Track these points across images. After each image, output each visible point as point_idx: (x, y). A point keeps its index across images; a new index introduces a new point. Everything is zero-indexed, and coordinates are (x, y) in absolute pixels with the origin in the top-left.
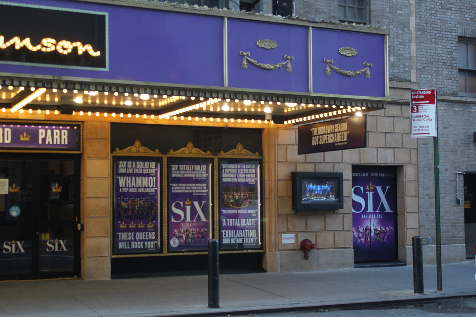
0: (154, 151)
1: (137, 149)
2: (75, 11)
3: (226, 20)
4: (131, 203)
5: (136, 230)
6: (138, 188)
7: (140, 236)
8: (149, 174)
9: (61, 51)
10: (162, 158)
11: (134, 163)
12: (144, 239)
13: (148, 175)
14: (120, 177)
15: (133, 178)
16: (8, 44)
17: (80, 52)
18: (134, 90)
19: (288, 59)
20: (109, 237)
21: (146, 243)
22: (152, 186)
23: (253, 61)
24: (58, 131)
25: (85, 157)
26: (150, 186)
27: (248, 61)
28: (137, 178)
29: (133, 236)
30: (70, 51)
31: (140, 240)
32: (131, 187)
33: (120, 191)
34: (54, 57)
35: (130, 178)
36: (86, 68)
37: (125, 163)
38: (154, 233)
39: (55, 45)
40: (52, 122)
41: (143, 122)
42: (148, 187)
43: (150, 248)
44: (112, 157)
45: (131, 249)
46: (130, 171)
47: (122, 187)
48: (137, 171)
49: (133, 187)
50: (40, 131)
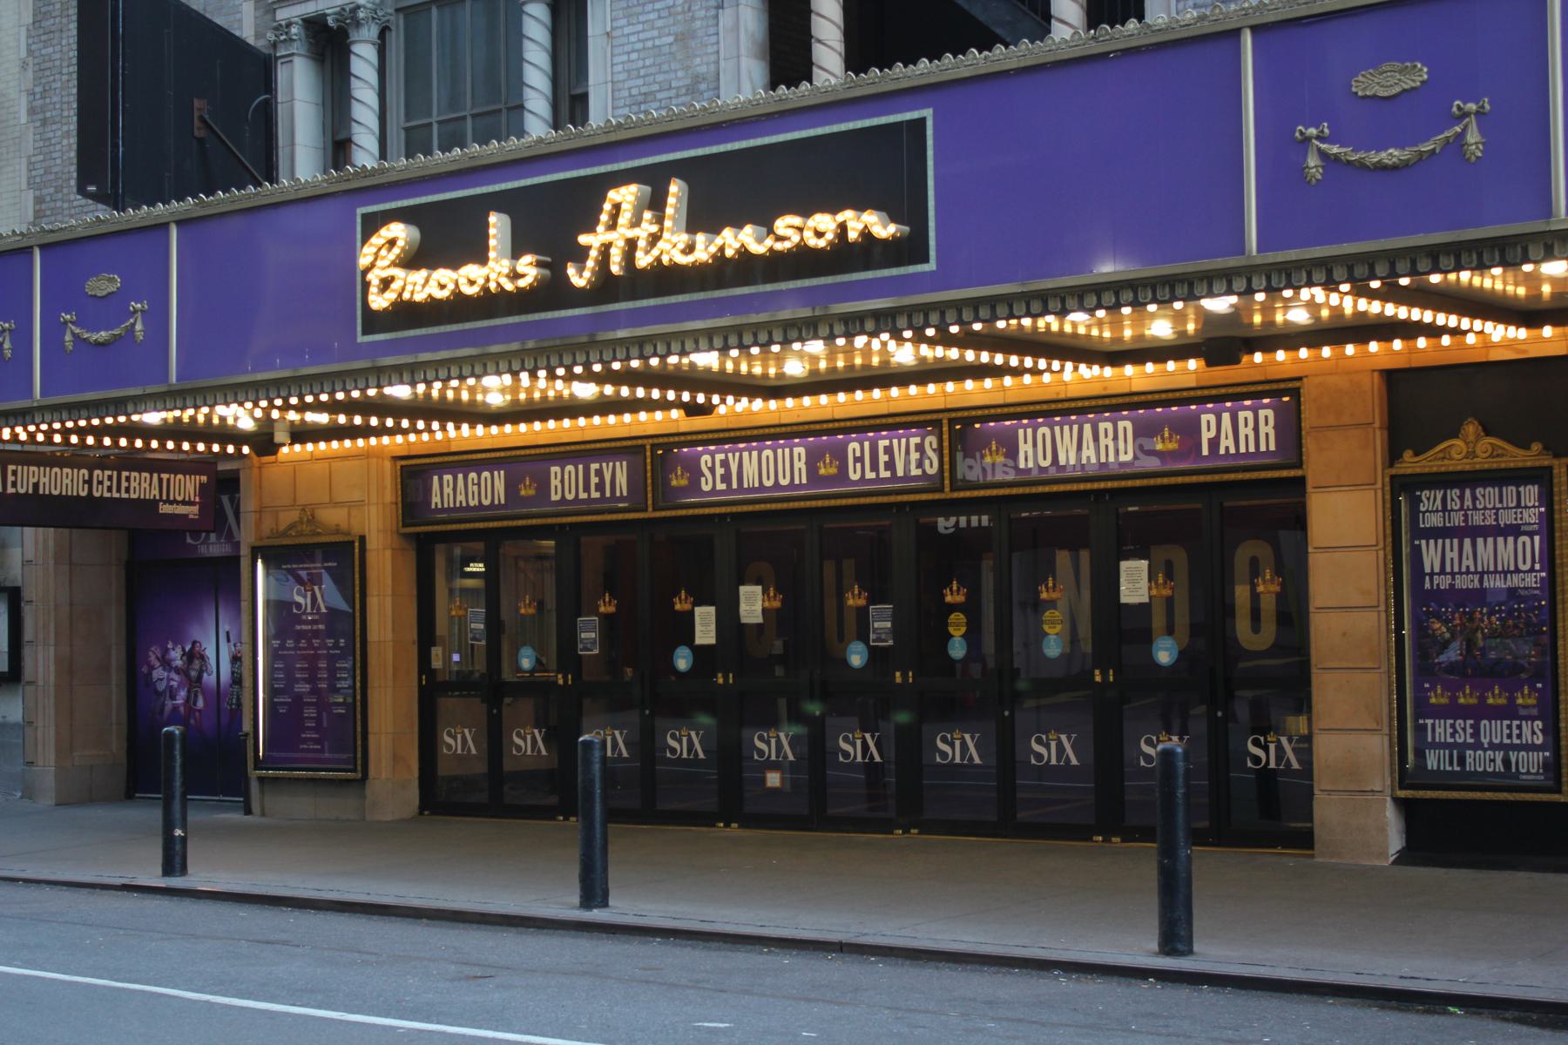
0: (1527, 448)
1: (1468, 447)
2: (820, 131)
3: (1247, 39)
4: (1463, 624)
5: (1480, 712)
6: (1482, 574)
7: (1494, 730)
8: (1519, 526)
9: (812, 242)
10: (1550, 468)
11: (1468, 492)
12: (1506, 741)
13: (1514, 531)
14: (1423, 542)
15: (1467, 542)
16: (713, 249)
17: (853, 235)
18: (1070, 303)
19: (1466, 115)
20: (1386, 730)
21: (1513, 756)
22: (1527, 567)
23: (1335, 149)
24: (1249, 414)
25: (1309, 489)
26: (1522, 567)
27: (1323, 155)
28: (1480, 541)
29: (1469, 731)
30: (830, 236)
31: (1493, 747)
32: (1461, 573)
33: (1427, 586)
34: (802, 261)
35: (1456, 541)
36: (886, 273)
37: (1439, 495)
38: (1539, 724)
39: (801, 230)
40: (1223, 391)
41: (1417, 362)
42: (1517, 570)
43: (1528, 773)
44: (1387, 480)
45: (1464, 774)
46: (1457, 520)
47: (1432, 574)
48: (1477, 519)
49: (1468, 572)
50: (1207, 418)
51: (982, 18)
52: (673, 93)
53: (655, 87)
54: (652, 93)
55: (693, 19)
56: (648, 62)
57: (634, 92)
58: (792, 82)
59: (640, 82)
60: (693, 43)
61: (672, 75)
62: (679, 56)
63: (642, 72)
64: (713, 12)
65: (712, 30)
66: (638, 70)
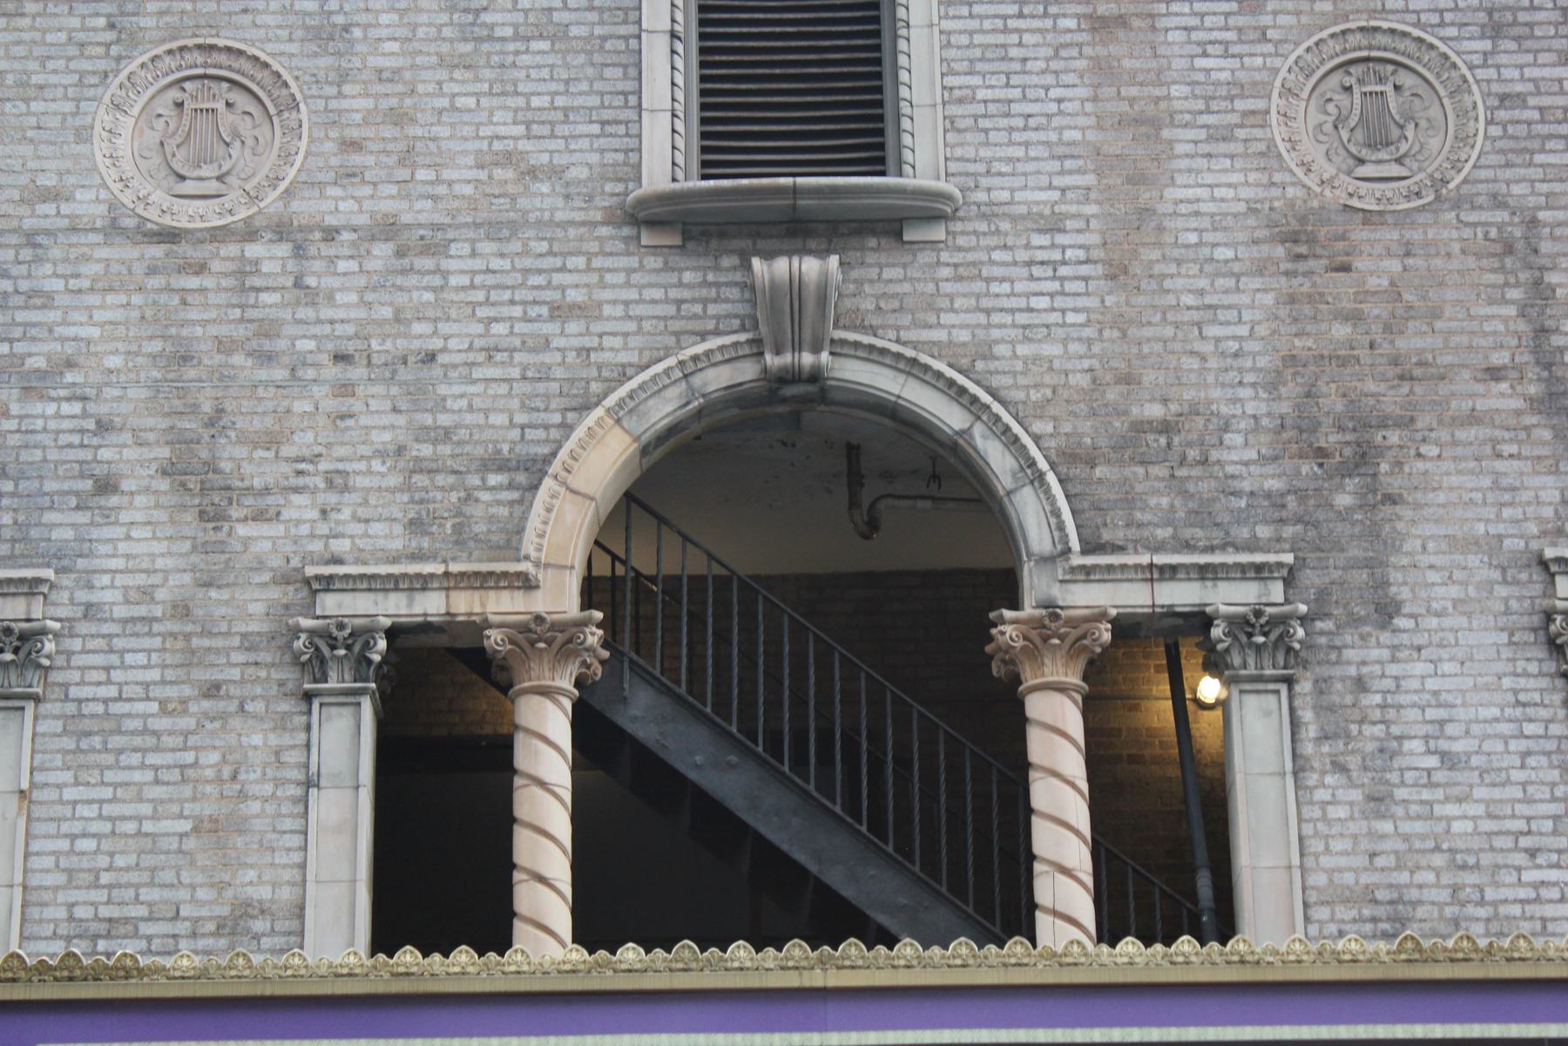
51: (848, 892)
52: (183, 928)
53: (143, 911)
54: (127, 920)
55: (243, 796)
56: (120, 861)
57: (80, 912)
58: (436, 942)
59: (101, 896)
60: (239, 841)
61: (183, 894)
62: (201, 860)
63: (105, 878)
64: (295, 791)
65: (288, 824)
66: (96, 873)
